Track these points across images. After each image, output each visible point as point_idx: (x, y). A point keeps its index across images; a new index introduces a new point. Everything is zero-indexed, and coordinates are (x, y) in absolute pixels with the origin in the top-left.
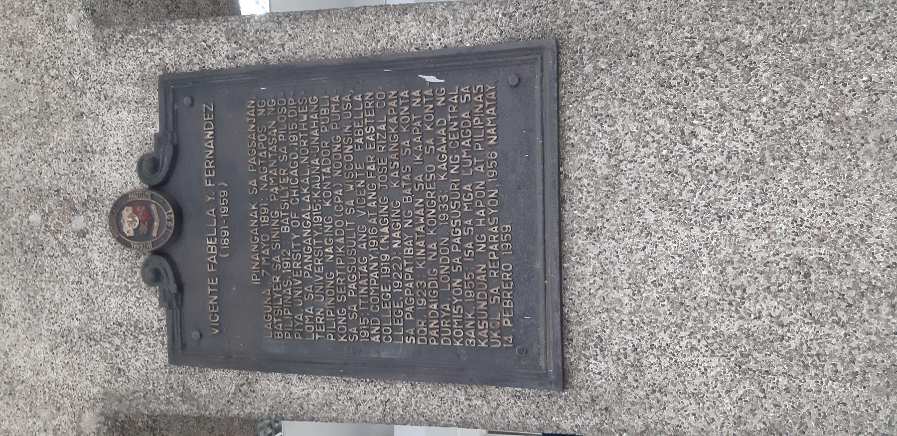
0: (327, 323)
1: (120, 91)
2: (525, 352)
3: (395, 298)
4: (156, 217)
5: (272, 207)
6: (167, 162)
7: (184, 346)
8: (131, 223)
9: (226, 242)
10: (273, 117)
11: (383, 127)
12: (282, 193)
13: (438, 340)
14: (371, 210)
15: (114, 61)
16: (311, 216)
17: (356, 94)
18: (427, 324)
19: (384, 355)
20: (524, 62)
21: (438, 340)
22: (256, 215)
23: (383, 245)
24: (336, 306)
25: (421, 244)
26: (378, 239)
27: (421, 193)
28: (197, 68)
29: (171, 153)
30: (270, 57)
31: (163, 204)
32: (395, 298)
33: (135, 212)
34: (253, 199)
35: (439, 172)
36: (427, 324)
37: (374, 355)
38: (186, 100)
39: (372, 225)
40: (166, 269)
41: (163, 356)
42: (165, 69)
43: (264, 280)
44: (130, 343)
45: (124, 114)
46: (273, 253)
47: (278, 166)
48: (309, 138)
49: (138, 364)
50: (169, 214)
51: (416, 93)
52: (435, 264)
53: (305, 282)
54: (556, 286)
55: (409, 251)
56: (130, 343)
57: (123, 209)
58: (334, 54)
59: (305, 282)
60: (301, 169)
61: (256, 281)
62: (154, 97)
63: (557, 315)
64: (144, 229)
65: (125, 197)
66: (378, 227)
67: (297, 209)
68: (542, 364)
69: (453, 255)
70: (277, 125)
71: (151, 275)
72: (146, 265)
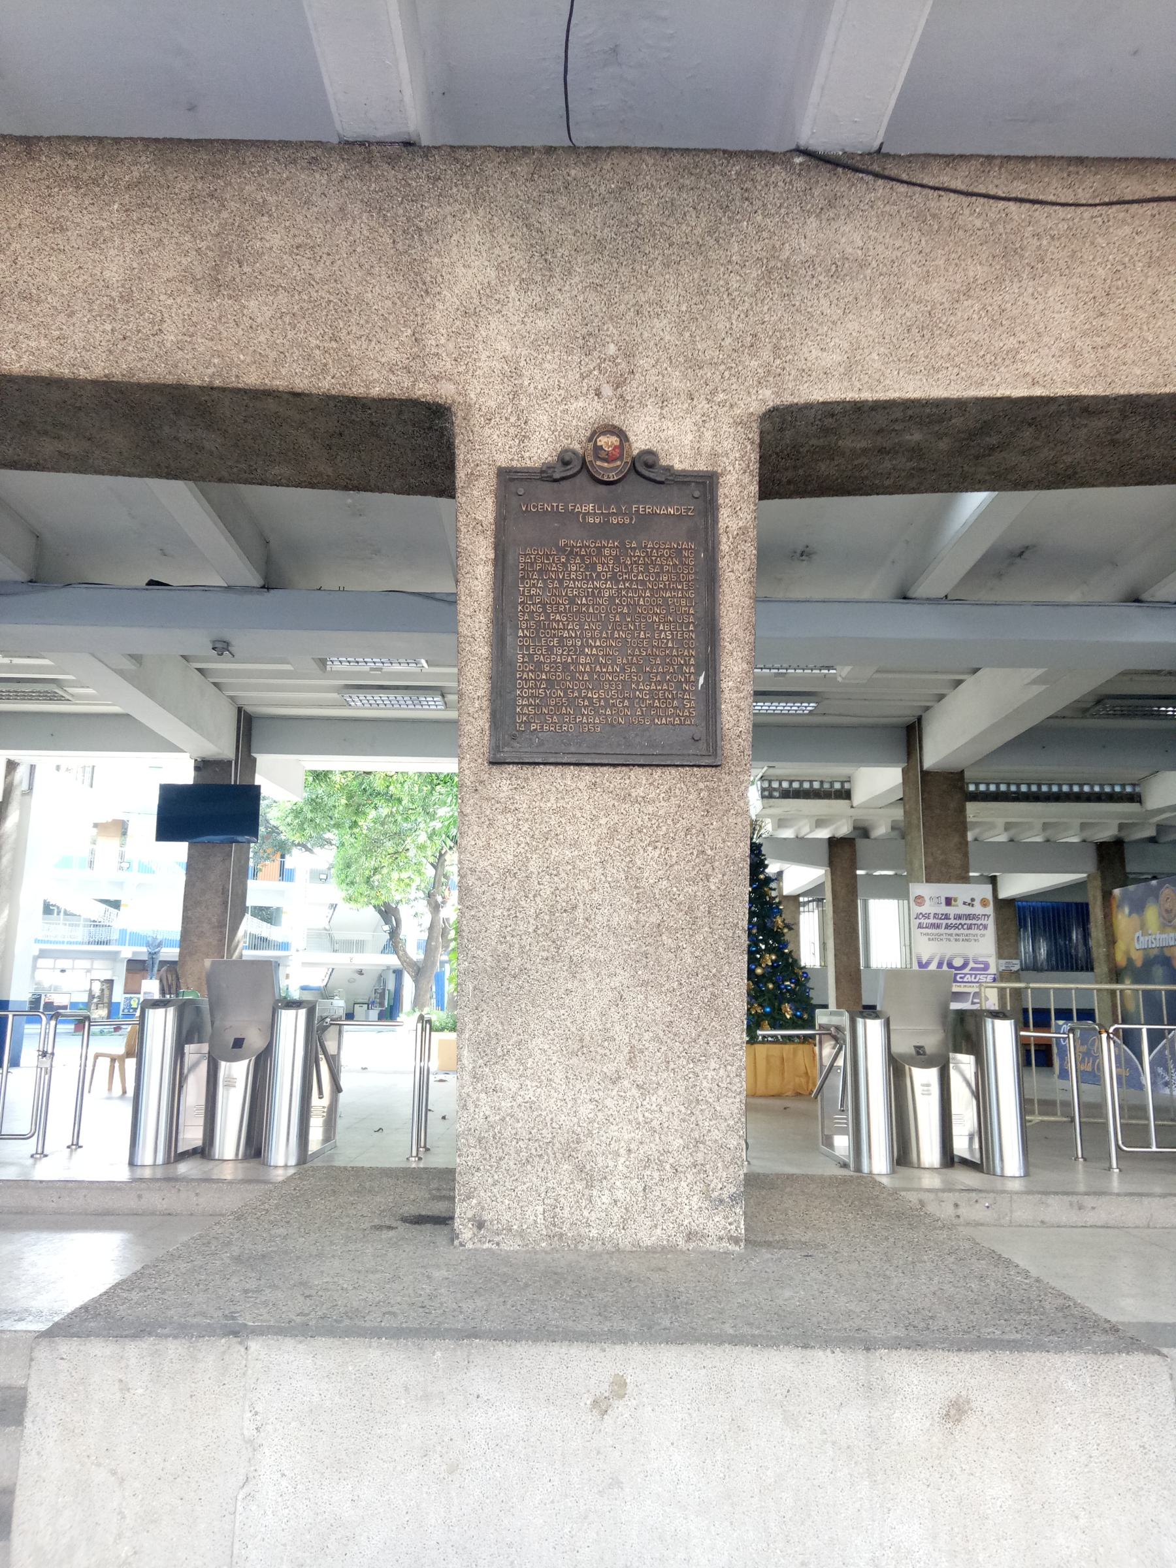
0: (531, 596)
1: (708, 434)
2: (514, 738)
3: (550, 649)
4: (611, 465)
5: (616, 558)
6: (652, 475)
7: (512, 480)
8: (607, 443)
9: (591, 520)
10: (681, 562)
11: (670, 645)
12: (626, 567)
13: (521, 678)
14: (612, 633)
15: (732, 430)
16: (609, 589)
17: (695, 627)
18: (531, 671)
19: (509, 639)
20: (708, 744)
21: (521, 678)
22: (610, 547)
23: (587, 641)
24: (544, 605)
25: (588, 669)
26: (591, 638)
27: (623, 670)
28: (721, 501)
29: (658, 479)
30: (725, 560)
31: (621, 471)
32: (550, 649)
33: (616, 447)
34: (623, 544)
35: (638, 684)
36: (531, 671)
37: (508, 631)
38: (697, 494)
39: (601, 633)
40: (570, 469)
41: (503, 460)
42: (722, 475)
43: (562, 550)
44: (512, 430)
45: (690, 437)
46: (582, 557)
47: (646, 565)
48: (665, 589)
49: (495, 437)
50: (613, 477)
51: (692, 670)
52: (573, 678)
53: (561, 582)
54: (559, 760)
55: (582, 660)
56: (512, 430)
57: (618, 436)
58: (723, 610)
59: (561, 582)
60: (643, 582)
61: (562, 543)
62: (702, 466)
63: (540, 760)
64: (603, 455)
65: (627, 440)
66: (600, 638)
67: (614, 578)
68: (506, 749)
69: (580, 691)
70: (675, 565)
71: (567, 458)
72: (574, 452)
